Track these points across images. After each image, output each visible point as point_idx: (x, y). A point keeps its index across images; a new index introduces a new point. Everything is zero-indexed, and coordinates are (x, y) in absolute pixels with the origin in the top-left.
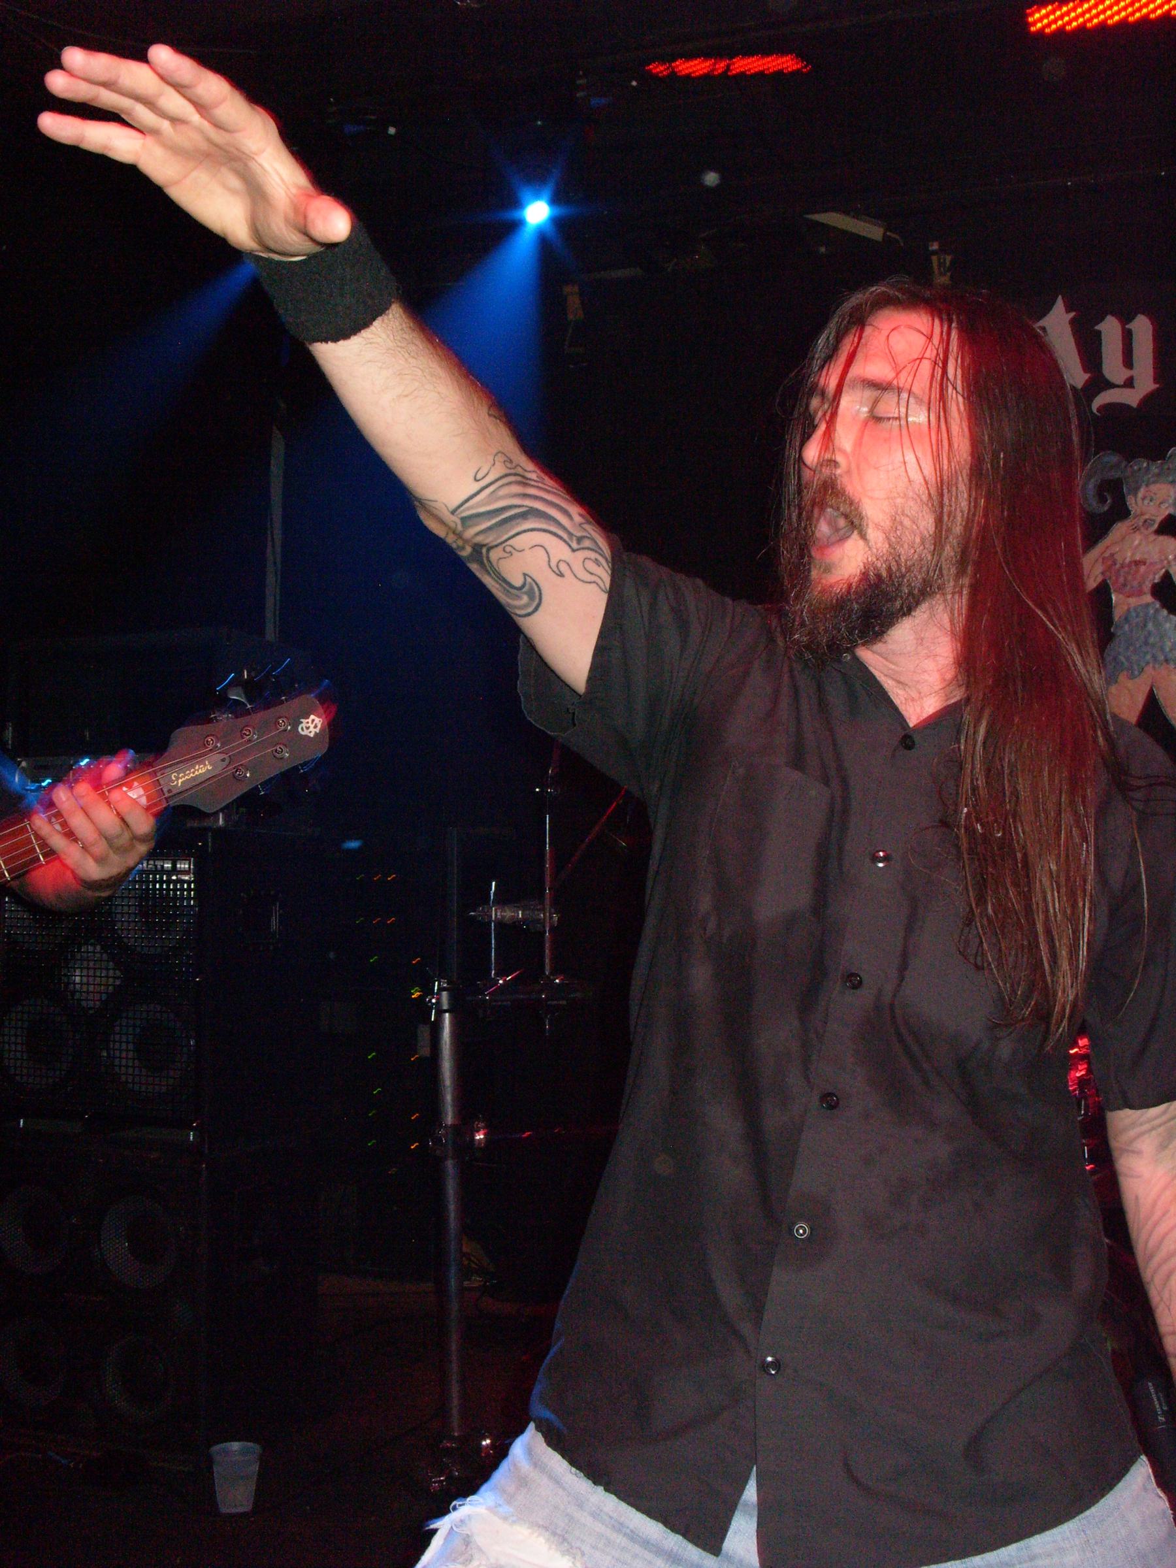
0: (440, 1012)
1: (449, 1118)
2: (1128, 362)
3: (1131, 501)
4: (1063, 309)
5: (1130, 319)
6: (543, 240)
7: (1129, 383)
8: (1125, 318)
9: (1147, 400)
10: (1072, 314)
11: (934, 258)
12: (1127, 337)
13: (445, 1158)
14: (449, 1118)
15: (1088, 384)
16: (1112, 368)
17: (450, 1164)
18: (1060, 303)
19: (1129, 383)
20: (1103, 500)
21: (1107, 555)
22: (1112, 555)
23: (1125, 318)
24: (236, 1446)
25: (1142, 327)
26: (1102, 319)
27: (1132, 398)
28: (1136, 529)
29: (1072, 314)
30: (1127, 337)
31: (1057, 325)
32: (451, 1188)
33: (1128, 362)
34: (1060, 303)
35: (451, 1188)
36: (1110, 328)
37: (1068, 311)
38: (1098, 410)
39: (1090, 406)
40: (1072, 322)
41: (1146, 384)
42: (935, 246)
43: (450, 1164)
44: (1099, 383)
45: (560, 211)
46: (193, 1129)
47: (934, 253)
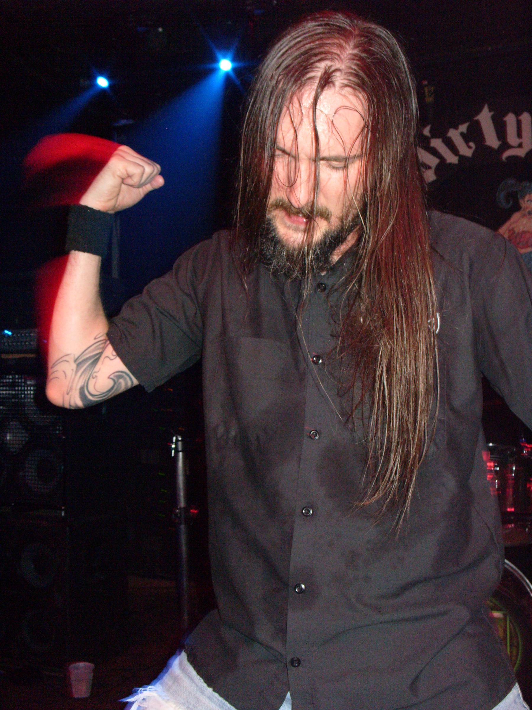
0: (177, 452)
1: (182, 503)
6: (227, 77)
7: (520, 146)
8: (518, 114)
10: (492, 113)
11: (426, 90)
12: (519, 124)
13: (180, 524)
14: (182, 503)
15: (500, 147)
16: (512, 138)
17: (183, 527)
18: (486, 109)
19: (520, 146)
20: (508, 202)
21: (511, 228)
22: (513, 228)
23: (518, 114)
24: (82, 664)
27: (521, 153)
28: (524, 216)
29: (492, 113)
30: (519, 124)
31: (485, 117)
32: (183, 539)
33: (519, 135)
34: (486, 109)
35: (183, 539)
36: (510, 119)
37: (490, 111)
42: (426, 83)
43: (183, 527)
44: (505, 146)
45: (237, 65)
46: (63, 510)
47: (426, 86)
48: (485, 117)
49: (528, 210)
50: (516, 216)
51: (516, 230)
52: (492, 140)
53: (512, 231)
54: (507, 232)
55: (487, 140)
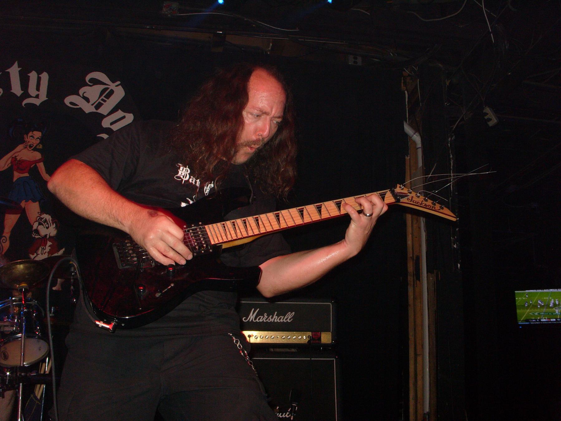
2: (38, 89)
3: (25, 136)
4: (17, 66)
5: (41, 73)
7: (37, 97)
8: (39, 73)
9: (43, 103)
10: (20, 69)
12: (39, 79)
16: (32, 90)
18: (16, 64)
19: (37, 97)
23: (39, 73)
25: (45, 77)
26: (31, 72)
27: (37, 102)
29: (20, 69)
30: (39, 79)
31: (14, 71)
33: (38, 89)
34: (16, 64)
36: (33, 75)
38: (25, 105)
39: (22, 104)
40: (20, 71)
41: (43, 97)
44: (26, 95)
48: (14, 71)
49: (29, 144)
50: (20, 147)
51: (18, 158)
52: (17, 90)
53: (14, 159)
54: (11, 159)
55: (13, 88)
